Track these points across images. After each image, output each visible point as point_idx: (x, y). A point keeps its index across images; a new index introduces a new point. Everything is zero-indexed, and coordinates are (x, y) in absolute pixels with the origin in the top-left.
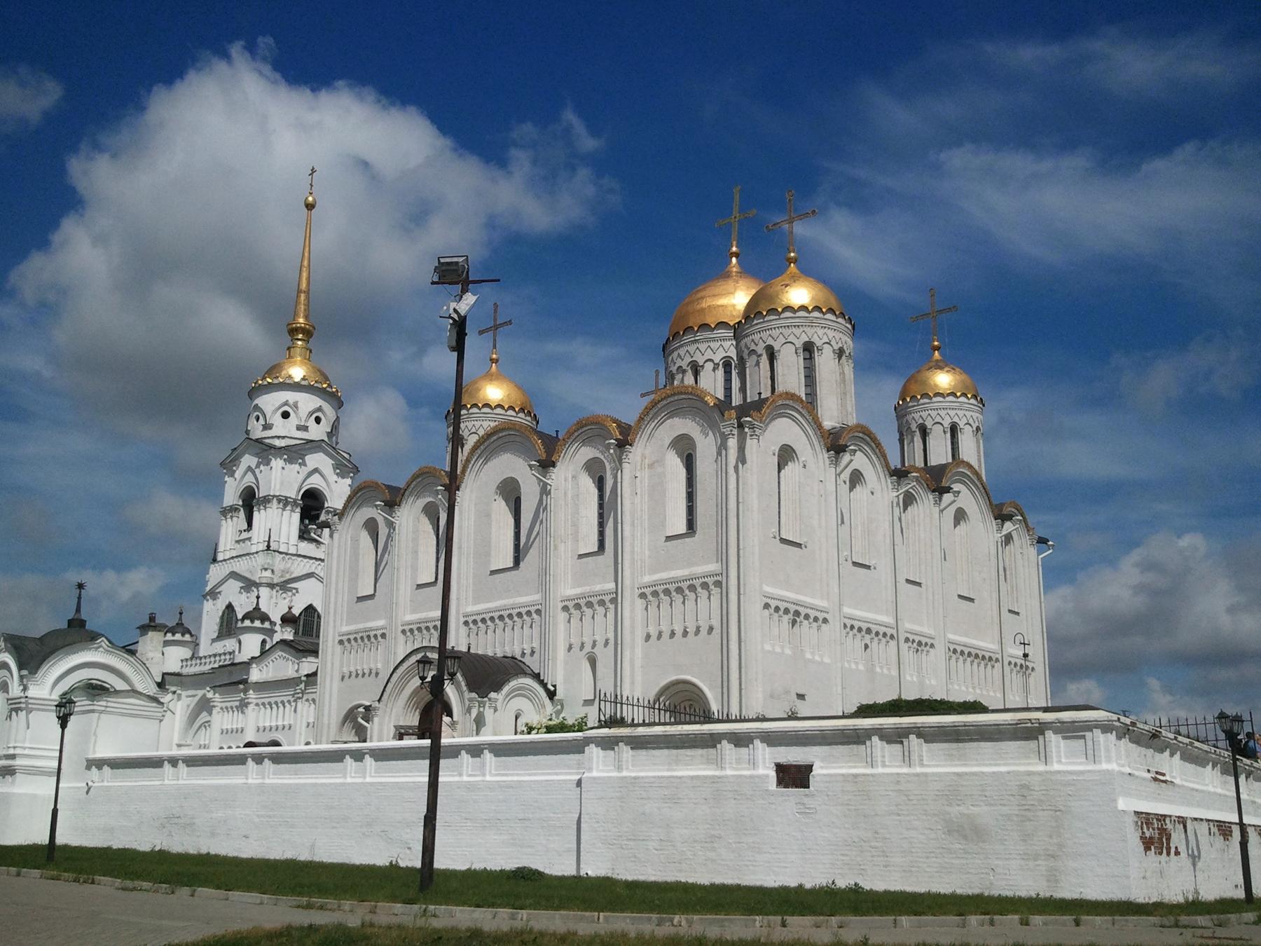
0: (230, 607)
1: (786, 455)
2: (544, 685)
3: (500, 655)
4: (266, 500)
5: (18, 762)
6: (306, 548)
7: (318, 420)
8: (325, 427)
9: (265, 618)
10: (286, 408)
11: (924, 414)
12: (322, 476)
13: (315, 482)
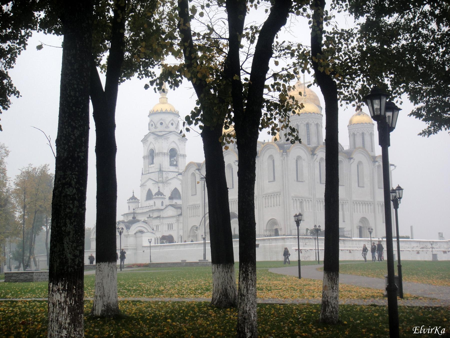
0: (149, 192)
1: (298, 158)
4: (159, 154)
5: (129, 247)
7: (172, 124)
8: (174, 126)
9: (162, 194)
10: (161, 121)
12: (175, 143)
13: (173, 146)
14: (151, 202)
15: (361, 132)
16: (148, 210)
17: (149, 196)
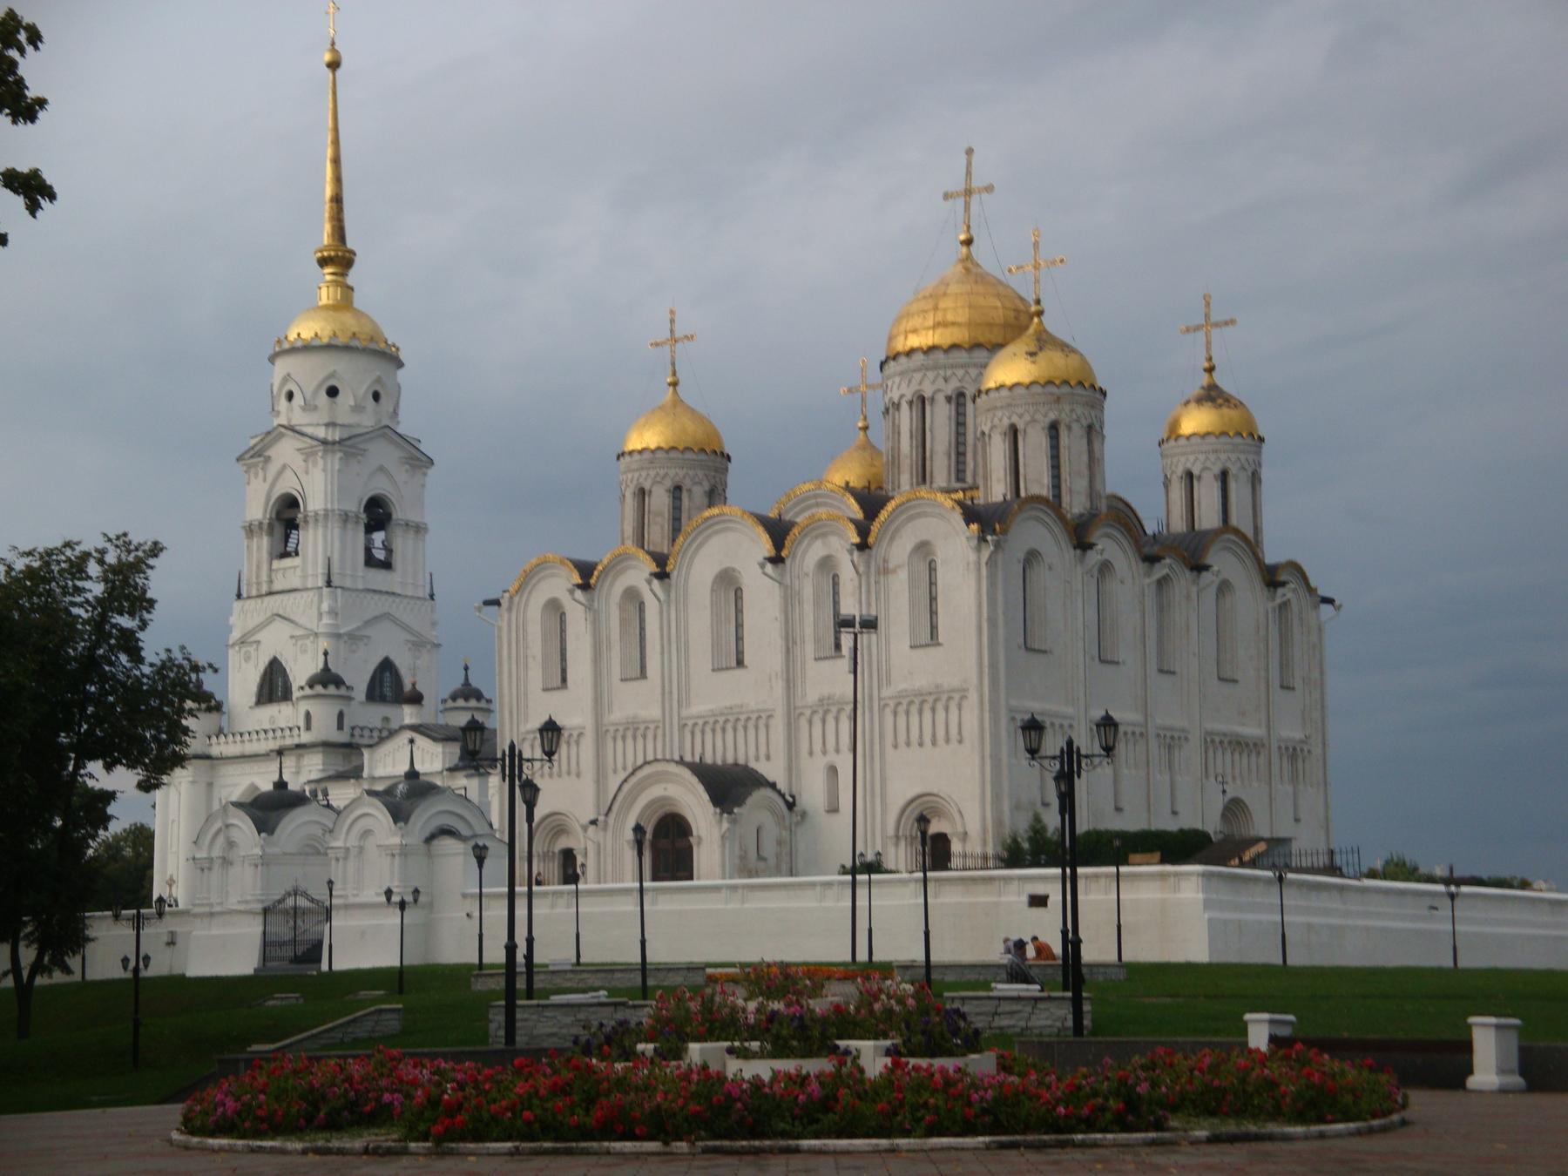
1: (1032, 557)
2: (783, 796)
3: (730, 760)
6: (378, 578)
7: (376, 396)
9: (338, 682)
10: (332, 382)
11: (1192, 458)
13: (380, 487)
14: (283, 715)
15: (1217, 469)
16: (273, 745)
17: (274, 686)
